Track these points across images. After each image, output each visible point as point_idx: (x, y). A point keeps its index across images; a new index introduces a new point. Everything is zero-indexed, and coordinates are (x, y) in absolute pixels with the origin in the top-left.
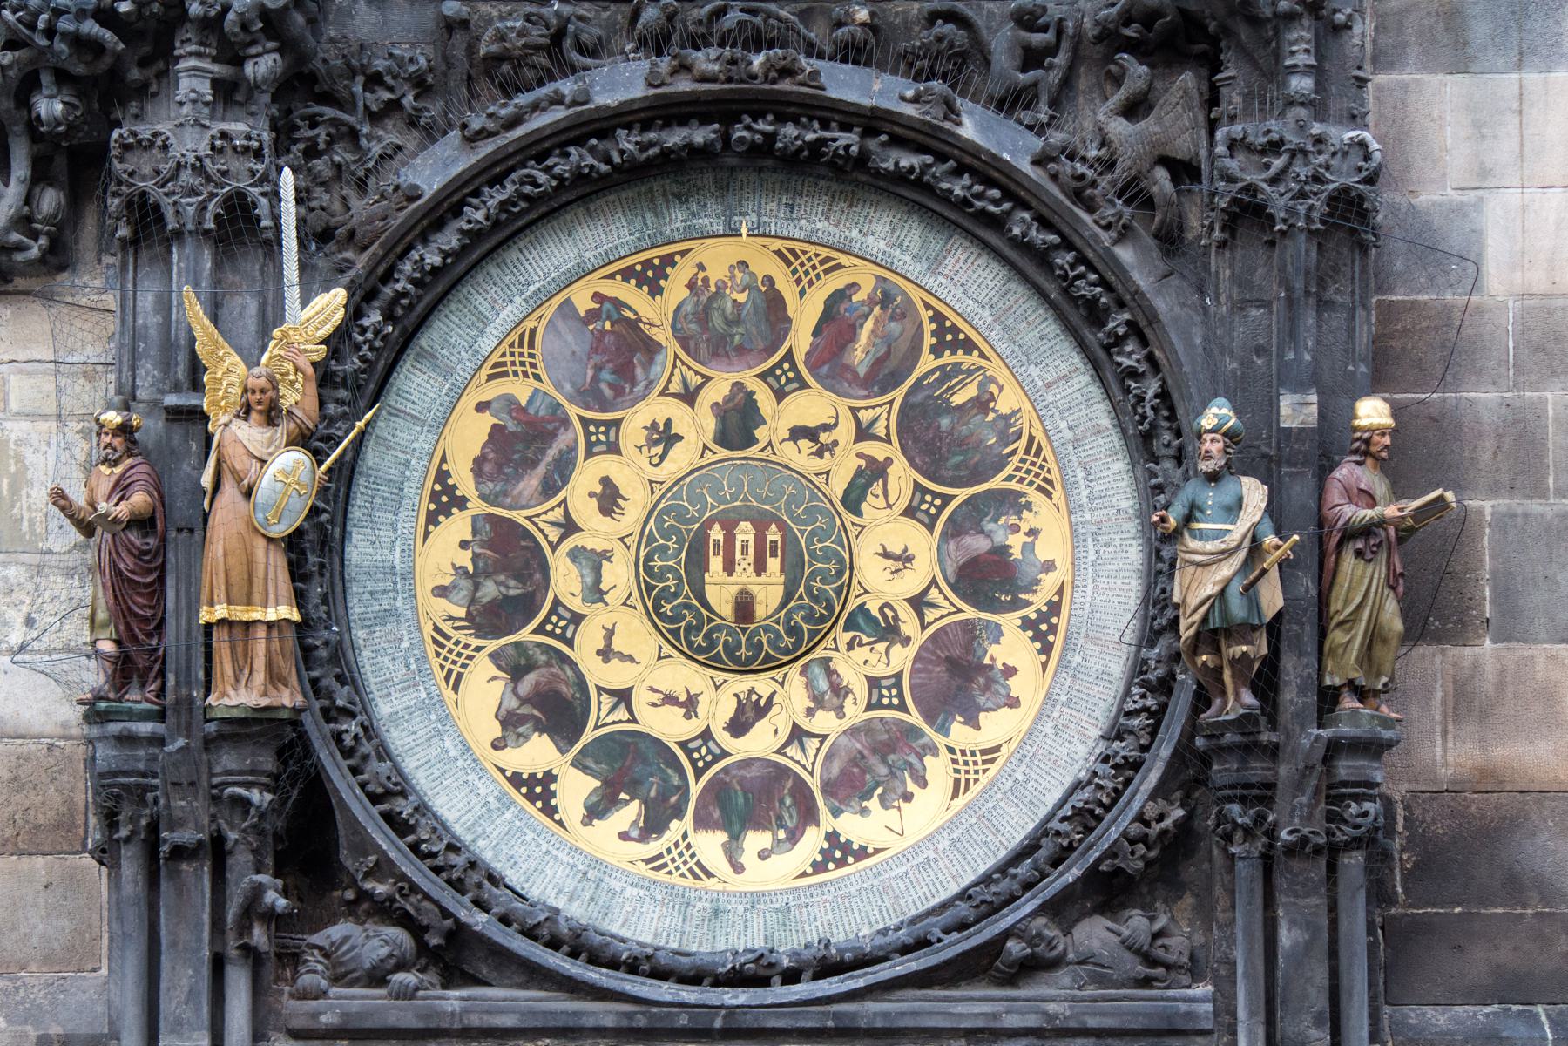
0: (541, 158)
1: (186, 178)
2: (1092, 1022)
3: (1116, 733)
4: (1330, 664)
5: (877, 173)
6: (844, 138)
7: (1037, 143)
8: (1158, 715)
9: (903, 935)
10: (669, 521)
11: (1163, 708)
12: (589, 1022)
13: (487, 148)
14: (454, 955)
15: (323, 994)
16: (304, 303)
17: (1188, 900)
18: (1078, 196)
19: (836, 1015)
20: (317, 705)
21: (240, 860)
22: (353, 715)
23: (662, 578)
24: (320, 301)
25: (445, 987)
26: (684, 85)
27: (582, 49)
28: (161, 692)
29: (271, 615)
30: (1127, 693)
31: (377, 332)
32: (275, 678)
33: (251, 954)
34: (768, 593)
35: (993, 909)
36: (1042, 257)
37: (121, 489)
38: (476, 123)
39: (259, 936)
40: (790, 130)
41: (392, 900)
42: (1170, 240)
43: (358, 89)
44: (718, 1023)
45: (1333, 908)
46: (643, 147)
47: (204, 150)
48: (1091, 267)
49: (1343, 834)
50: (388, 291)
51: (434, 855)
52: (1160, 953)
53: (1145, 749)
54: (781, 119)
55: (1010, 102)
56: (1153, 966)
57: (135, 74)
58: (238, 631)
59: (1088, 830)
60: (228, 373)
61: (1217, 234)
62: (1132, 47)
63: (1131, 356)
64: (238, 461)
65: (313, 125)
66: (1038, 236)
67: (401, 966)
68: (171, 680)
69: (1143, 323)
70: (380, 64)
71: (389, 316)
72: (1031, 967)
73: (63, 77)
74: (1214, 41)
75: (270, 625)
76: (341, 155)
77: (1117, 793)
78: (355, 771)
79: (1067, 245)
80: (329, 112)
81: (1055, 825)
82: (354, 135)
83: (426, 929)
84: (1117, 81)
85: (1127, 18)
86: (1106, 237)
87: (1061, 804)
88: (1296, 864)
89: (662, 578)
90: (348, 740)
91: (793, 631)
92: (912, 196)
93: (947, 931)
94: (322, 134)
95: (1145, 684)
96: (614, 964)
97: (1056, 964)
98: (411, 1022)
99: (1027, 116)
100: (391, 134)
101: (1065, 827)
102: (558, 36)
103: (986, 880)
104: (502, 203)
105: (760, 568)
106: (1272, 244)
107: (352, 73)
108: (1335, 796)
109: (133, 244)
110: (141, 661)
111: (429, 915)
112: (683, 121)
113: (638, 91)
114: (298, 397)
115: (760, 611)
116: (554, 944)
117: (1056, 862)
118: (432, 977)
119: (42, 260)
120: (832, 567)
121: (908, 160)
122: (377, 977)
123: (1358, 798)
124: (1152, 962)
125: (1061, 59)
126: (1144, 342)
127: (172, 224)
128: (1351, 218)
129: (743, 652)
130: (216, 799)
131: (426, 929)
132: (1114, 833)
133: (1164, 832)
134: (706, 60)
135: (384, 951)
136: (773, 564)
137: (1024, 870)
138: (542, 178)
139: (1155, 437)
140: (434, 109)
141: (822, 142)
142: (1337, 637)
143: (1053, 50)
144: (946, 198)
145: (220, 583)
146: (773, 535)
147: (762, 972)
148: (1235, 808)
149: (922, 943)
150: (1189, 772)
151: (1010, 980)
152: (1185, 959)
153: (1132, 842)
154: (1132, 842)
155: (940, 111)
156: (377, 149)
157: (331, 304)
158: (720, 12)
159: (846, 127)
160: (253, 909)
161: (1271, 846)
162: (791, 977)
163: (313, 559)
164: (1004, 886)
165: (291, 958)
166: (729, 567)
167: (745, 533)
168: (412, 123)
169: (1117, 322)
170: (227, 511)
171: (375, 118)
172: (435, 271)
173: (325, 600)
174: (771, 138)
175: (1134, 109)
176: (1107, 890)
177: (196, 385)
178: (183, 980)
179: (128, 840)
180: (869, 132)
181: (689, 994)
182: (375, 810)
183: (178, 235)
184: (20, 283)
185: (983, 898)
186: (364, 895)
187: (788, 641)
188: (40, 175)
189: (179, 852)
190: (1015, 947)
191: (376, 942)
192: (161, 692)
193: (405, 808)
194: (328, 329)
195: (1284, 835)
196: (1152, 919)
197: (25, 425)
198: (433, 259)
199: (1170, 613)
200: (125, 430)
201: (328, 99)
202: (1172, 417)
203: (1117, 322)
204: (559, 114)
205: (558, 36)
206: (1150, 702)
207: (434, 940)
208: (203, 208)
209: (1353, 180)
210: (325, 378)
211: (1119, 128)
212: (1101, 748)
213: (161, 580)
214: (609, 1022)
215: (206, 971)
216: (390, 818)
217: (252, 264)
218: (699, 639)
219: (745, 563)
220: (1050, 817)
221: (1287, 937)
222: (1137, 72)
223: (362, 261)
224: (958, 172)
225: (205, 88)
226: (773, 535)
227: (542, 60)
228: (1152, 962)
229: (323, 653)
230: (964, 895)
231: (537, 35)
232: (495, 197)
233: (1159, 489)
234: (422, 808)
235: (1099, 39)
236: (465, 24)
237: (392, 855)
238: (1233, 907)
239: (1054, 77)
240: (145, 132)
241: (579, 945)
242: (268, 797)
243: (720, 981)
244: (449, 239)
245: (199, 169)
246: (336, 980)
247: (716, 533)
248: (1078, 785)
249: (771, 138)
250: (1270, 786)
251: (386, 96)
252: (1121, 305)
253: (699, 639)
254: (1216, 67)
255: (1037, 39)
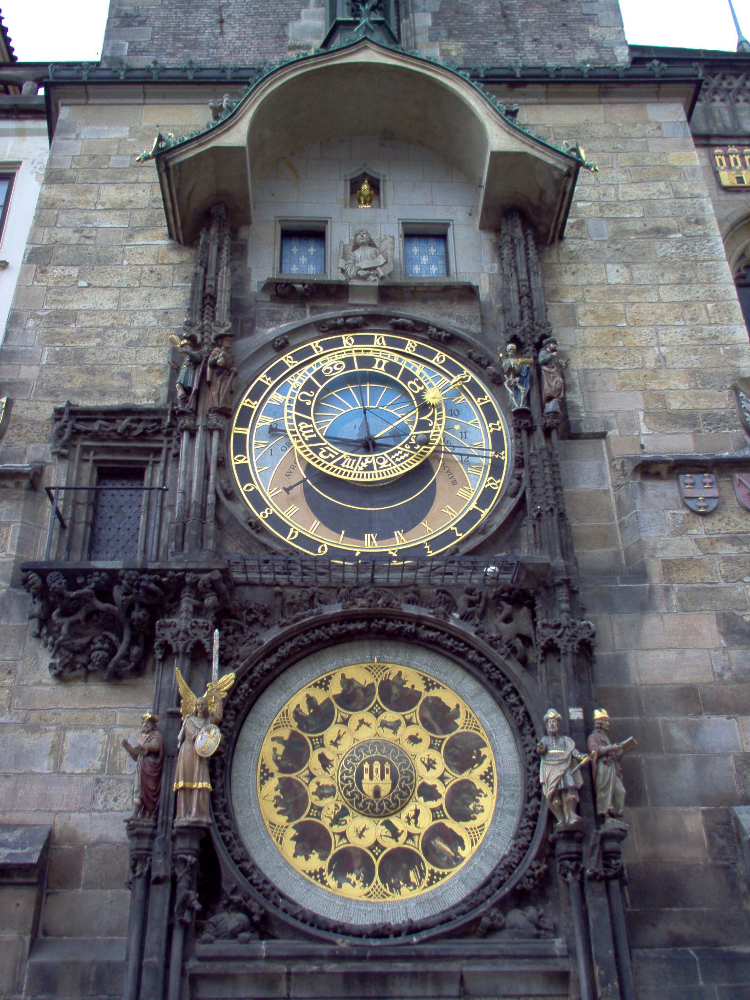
0: (305, 633)
1: (181, 635)
2: (518, 952)
3: (517, 836)
4: (599, 806)
5: (421, 640)
6: (409, 627)
7: (475, 629)
8: (533, 828)
9: (441, 918)
10: (349, 762)
11: (535, 826)
12: (318, 953)
13: (287, 628)
14: (263, 927)
15: (211, 942)
16: (220, 677)
17: (550, 903)
18: (491, 644)
19: (415, 950)
20: (216, 825)
21: (182, 884)
22: (229, 829)
23: (346, 782)
24: (224, 678)
25: (262, 938)
26: (354, 608)
27: (320, 602)
28: (156, 820)
29: (200, 785)
30: (521, 821)
31: (246, 691)
32: (200, 811)
33: (185, 926)
34: (386, 787)
35: (475, 906)
36: (479, 666)
37: (148, 740)
38: (284, 621)
39: (187, 917)
40: (391, 624)
41: (240, 902)
42: (524, 662)
43: (244, 613)
44: (369, 954)
45: (610, 902)
46: (341, 630)
47: (188, 626)
48: (497, 669)
49: (611, 873)
50: (251, 677)
51: (257, 884)
52: (541, 924)
53: (530, 842)
54: (388, 620)
55: (465, 617)
56: (539, 930)
57: (167, 605)
58: (188, 792)
59: (510, 874)
60: (192, 701)
61: (540, 658)
62: (507, 600)
63: (513, 699)
64: (190, 729)
65: (228, 624)
66: (477, 658)
67: (243, 930)
68: (161, 812)
69: (516, 687)
70: (252, 606)
71: (251, 686)
72: (491, 930)
73: (142, 605)
74: (533, 601)
75: (200, 790)
76: (237, 635)
77: (521, 859)
78: (230, 851)
79: (488, 661)
80: (234, 621)
81: (498, 871)
82: (241, 629)
83: (253, 914)
84: (500, 612)
85: (503, 591)
86: (502, 658)
87: (499, 864)
88: (594, 885)
89: (346, 782)
90: (227, 839)
91: (396, 801)
92: (432, 646)
93: (458, 915)
94: (231, 628)
95: (528, 816)
96: (327, 929)
97: (502, 928)
98: (248, 954)
99: (472, 622)
100: (256, 629)
101: (501, 872)
102: (312, 597)
103: (472, 895)
104: (292, 648)
105: (382, 777)
106: (559, 661)
107: (242, 609)
108: (607, 857)
109: (163, 660)
110: (150, 807)
111: (255, 908)
112: (354, 621)
113: (339, 610)
114: (216, 709)
115: (383, 794)
116: (304, 921)
117: (499, 886)
118: (256, 935)
119: (132, 670)
120: (408, 777)
121: (431, 634)
122: (233, 935)
123: (615, 858)
124: (539, 928)
125: (482, 604)
126: (517, 694)
127: (175, 650)
128: (586, 649)
129: (377, 809)
130: (174, 860)
131: (253, 914)
132: (521, 874)
133: (540, 874)
134: (361, 602)
135: (237, 923)
136: (387, 776)
137: (487, 890)
138: (306, 640)
139: (525, 726)
140: (270, 621)
141: (402, 628)
142: (600, 795)
143: (479, 601)
144: (445, 647)
145: (181, 776)
146: (387, 766)
147: (386, 932)
148: (567, 863)
149: (449, 920)
150: (548, 851)
151: (484, 936)
152: (552, 927)
153: (528, 877)
154: (528, 877)
155: (441, 618)
156: (250, 634)
157: (229, 679)
158: (366, 591)
159: (410, 623)
160: (186, 904)
161: (582, 878)
162: (397, 934)
163: (218, 771)
164: (481, 897)
165: (199, 929)
166: (371, 777)
167: (377, 765)
168: (263, 625)
169: (507, 687)
170: (184, 749)
171: (250, 624)
172: (268, 671)
173: (222, 787)
174: (384, 627)
175: (507, 620)
176: (519, 898)
177: (179, 705)
178: (155, 935)
179: (139, 877)
180: (418, 625)
181: (358, 941)
182: (237, 867)
183: (177, 654)
184: (125, 681)
185: (472, 902)
186: (230, 902)
187: (393, 805)
188: (133, 642)
189: (158, 881)
190: (485, 920)
191: (233, 920)
192: (156, 820)
193: (247, 866)
194: (228, 686)
195: (588, 871)
196: (538, 910)
197: (121, 730)
198: (267, 666)
199: (535, 790)
200: (152, 721)
201: (233, 617)
202: (529, 719)
203: (507, 687)
204: (312, 618)
205: (312, 597)
206: (530, 823)
207: (256, 918)
208: (186, 646)
209: (586, 636)
210: (227, 706)
211: (503, 625)
212: (513, 842)
213: (160, 776)
214: (325, 953)
215: (164, 930)
216: (242, 870)
217: (203, 667)
218: (361, 805)
219: (377, 776)
220: (496, 869)
221: (592, 915)
222: (507, 608)
223: (242, 665)
224: (449, 638)
225: (191, 609)
226: (387, 766)
227: (306, 605)
228: (539, 928)
229: (220, 806)
230: (464, 901)
231: (305, 597)
232: (290, 645)
233: (527, 745)
234: (254, 866)
235: (494, 597)
236: (281, 594)
237: (242, 883)
238: (570, 904)
239: (479, 610)
240: (168, 621)
241: (315, 921)
242: (194, 859)
243: (368, 937)
244: (273, 659)
245: (186, 632)
246: (217, 937)
247: (366, 766)
248: (505, 857)
249: (384, 627)
250: (580, 854)
251: (253, 616)
252: (509, 681)
253: (361, 805)
254: (535, 605)
255: (473, 598)
